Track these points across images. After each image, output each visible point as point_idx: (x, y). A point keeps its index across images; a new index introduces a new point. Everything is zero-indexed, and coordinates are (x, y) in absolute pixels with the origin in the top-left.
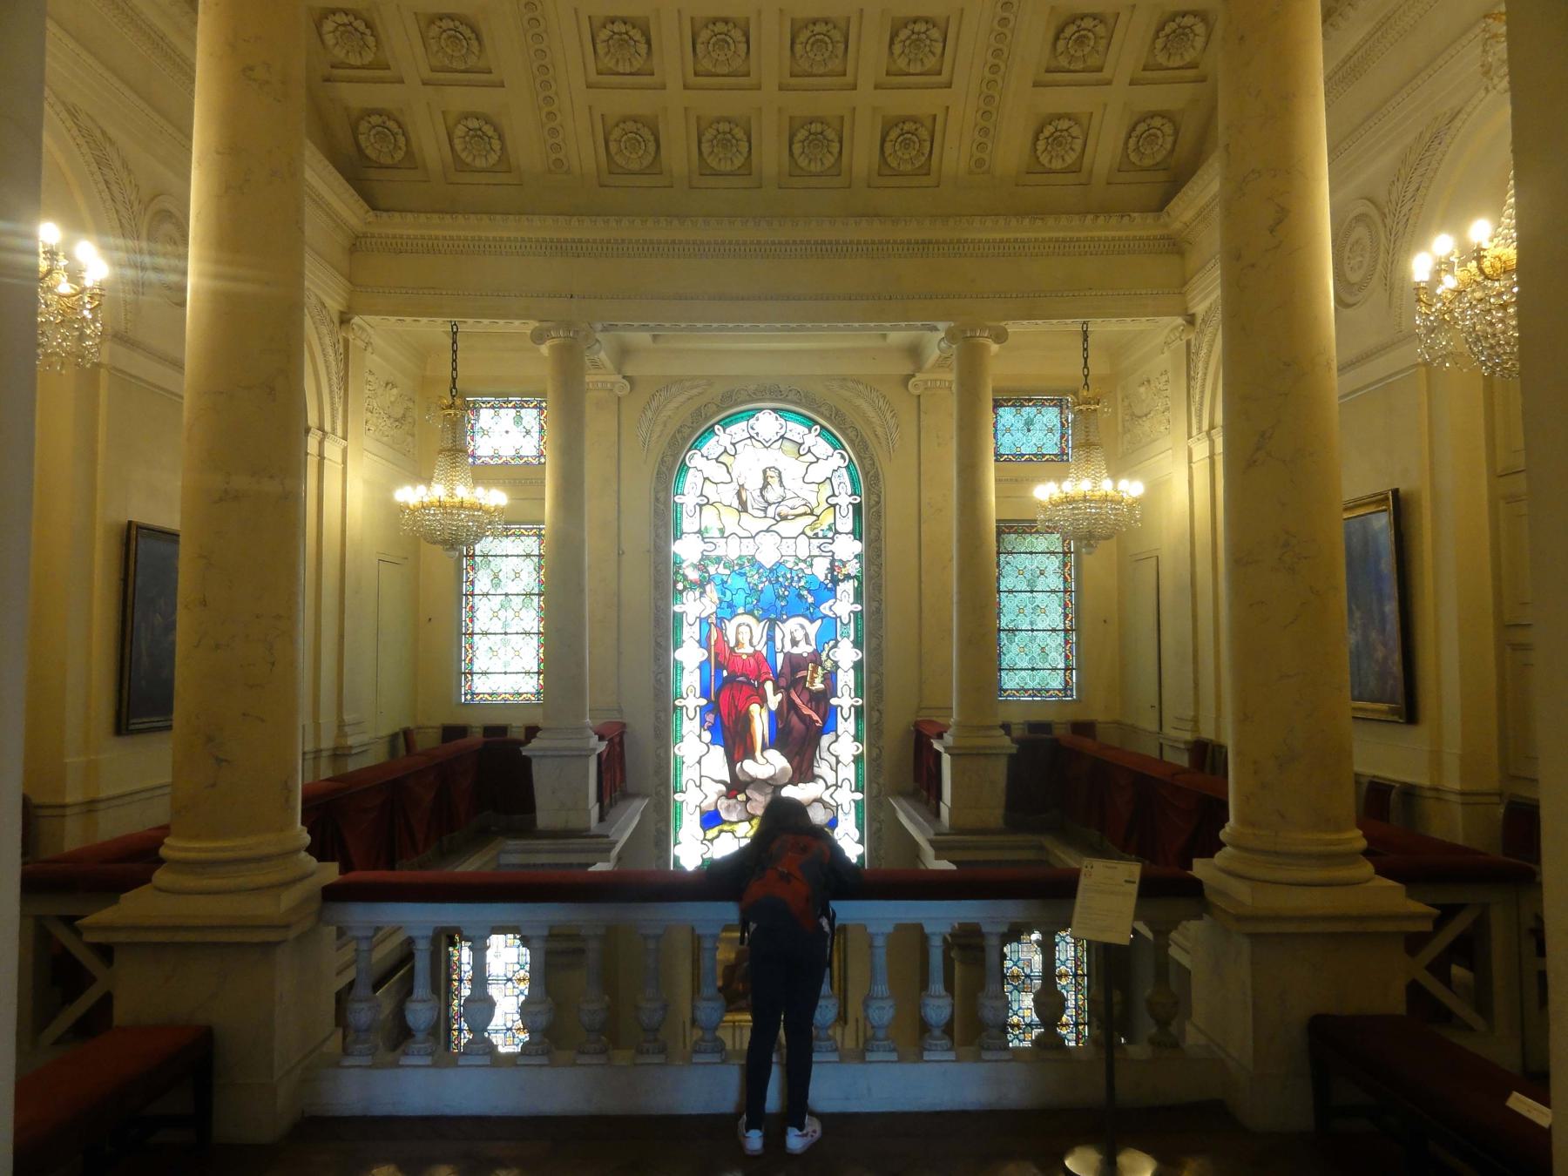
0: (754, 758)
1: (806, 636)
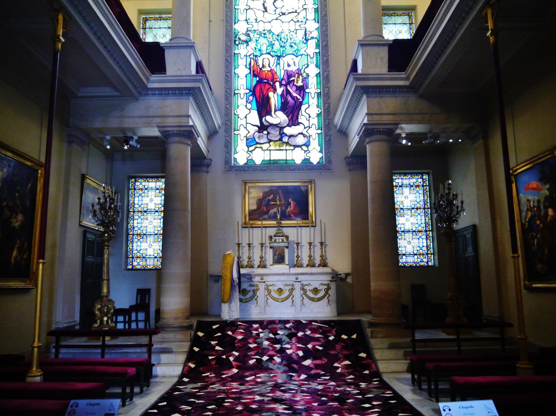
0: (271, 115)
1: (294, 62)
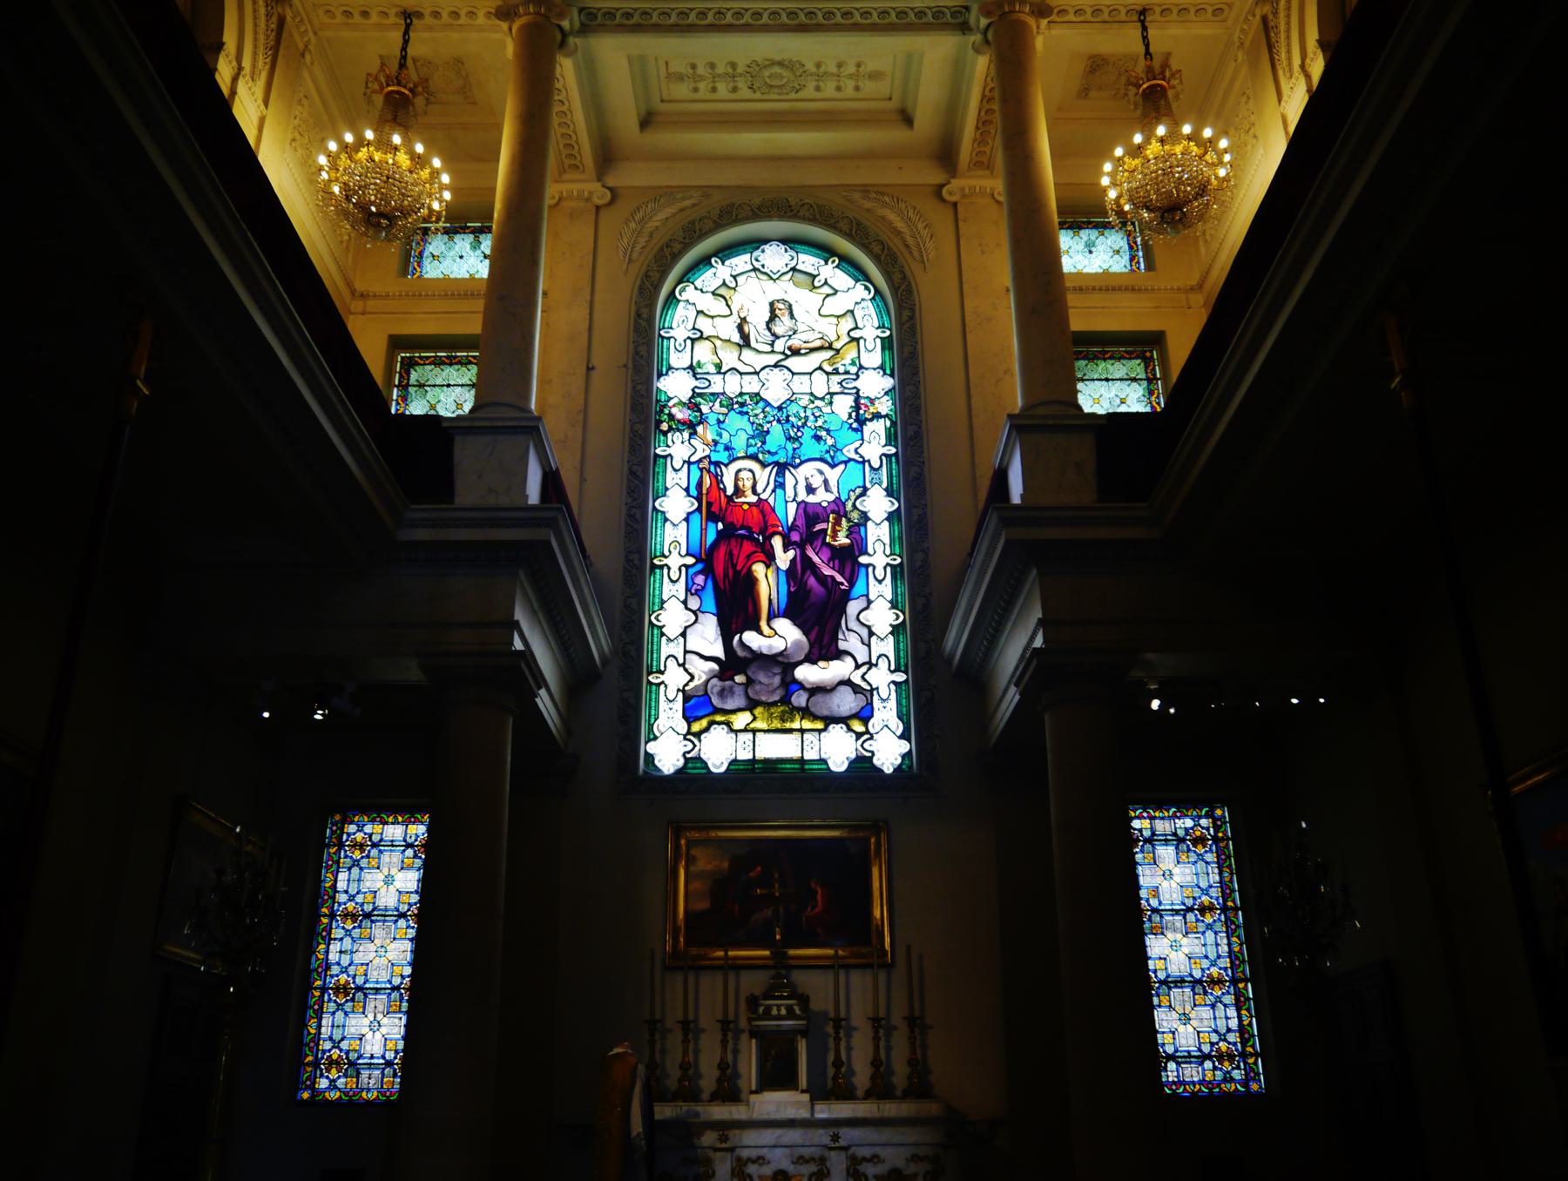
1: (826, 482)
